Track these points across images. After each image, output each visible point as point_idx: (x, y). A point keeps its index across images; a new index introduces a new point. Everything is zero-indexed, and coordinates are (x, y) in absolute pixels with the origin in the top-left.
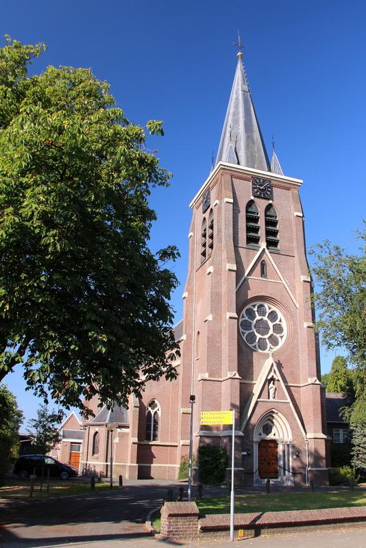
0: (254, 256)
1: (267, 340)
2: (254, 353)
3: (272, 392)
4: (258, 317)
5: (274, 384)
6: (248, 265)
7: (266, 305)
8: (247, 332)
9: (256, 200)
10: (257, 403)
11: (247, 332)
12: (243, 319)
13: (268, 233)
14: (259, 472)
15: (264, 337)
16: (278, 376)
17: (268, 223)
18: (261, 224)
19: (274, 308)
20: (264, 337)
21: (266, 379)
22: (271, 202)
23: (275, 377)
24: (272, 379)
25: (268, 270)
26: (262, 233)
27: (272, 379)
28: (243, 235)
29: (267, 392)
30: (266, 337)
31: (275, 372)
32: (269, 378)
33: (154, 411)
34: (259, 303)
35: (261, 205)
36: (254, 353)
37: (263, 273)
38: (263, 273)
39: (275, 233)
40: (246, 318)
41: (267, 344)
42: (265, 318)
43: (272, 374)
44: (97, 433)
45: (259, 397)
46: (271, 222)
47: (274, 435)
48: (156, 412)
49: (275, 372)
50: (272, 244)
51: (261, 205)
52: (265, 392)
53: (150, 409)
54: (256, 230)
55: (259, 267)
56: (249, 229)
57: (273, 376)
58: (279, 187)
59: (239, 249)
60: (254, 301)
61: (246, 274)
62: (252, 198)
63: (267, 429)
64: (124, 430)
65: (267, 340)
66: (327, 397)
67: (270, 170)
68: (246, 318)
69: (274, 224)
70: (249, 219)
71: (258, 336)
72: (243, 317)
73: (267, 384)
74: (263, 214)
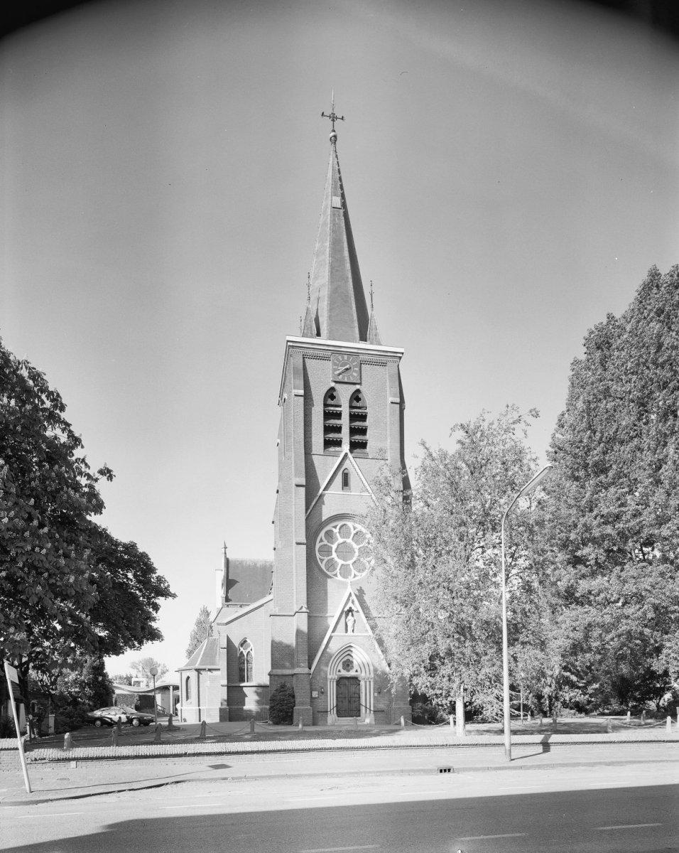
0: (333, 464)
1: (351, 566)
2: (329, 580)
3: (350, 624)
4: (341, 540)
5: (353, 615)
6: (324, 479)
7: (350, 524)
8: (326, 559)
9: (338, 387)
10: (331, 638)
11: (326, 559)
12: (322, 543)
13: (353, 431)
14: (337, 711)
15: (348, 563)
16: (356, 607)
17: (353, 417)
18: (345, 422)
19: (359, 527)
20: (348, 563)
21: (343, 611)
22: (358, 387)
23: (353, 608)
24: (350, 610)
25: (353, 480)
26: (345, 435)
27: (350, 610)
28: (318, 437)
29: (344, 624)
30: (350, 562)
31: (353, 602)
32: (346, 609)
33: (247, 651)
34: (340, 523)
35: (344, 394)
36: (329, 580)
37: (346, 483)
38: (346, 483)
39: (363, 431)
40: (325, 542)
41: (351, 570)
42: (349, 541)
43: (350, 605)
44: (188, 678)
45: (333, 631)
46: (358, 418)
47: (357, 671)
48: (249, 652)
49: (353, 602)
50: (358, 446)
51: (344, 394)
52: (341, 625)
53: (242, 649)
54: (338, 429)
55: (339, 478)
56: (328, 429)
57: (350, 608)
58: (370, 363)
59: (314, 457)
60: (335, 521)
61: (323, 487)
62: (333, 384)
63: (348, 665)
64: (215, 673)
65: (351, 566)
66: (218, 721)
67: (363, 338)
68: (325, 542)
69: (363, 418)
70: (328, 415)
71: (340, 562)
72: (321, 541)
73: (344, 616)
74: (348, 405)
